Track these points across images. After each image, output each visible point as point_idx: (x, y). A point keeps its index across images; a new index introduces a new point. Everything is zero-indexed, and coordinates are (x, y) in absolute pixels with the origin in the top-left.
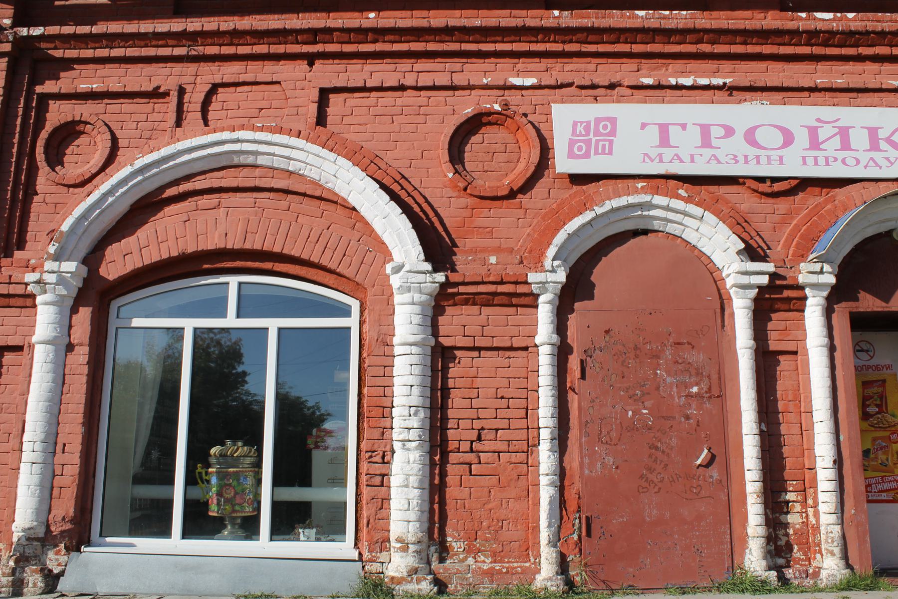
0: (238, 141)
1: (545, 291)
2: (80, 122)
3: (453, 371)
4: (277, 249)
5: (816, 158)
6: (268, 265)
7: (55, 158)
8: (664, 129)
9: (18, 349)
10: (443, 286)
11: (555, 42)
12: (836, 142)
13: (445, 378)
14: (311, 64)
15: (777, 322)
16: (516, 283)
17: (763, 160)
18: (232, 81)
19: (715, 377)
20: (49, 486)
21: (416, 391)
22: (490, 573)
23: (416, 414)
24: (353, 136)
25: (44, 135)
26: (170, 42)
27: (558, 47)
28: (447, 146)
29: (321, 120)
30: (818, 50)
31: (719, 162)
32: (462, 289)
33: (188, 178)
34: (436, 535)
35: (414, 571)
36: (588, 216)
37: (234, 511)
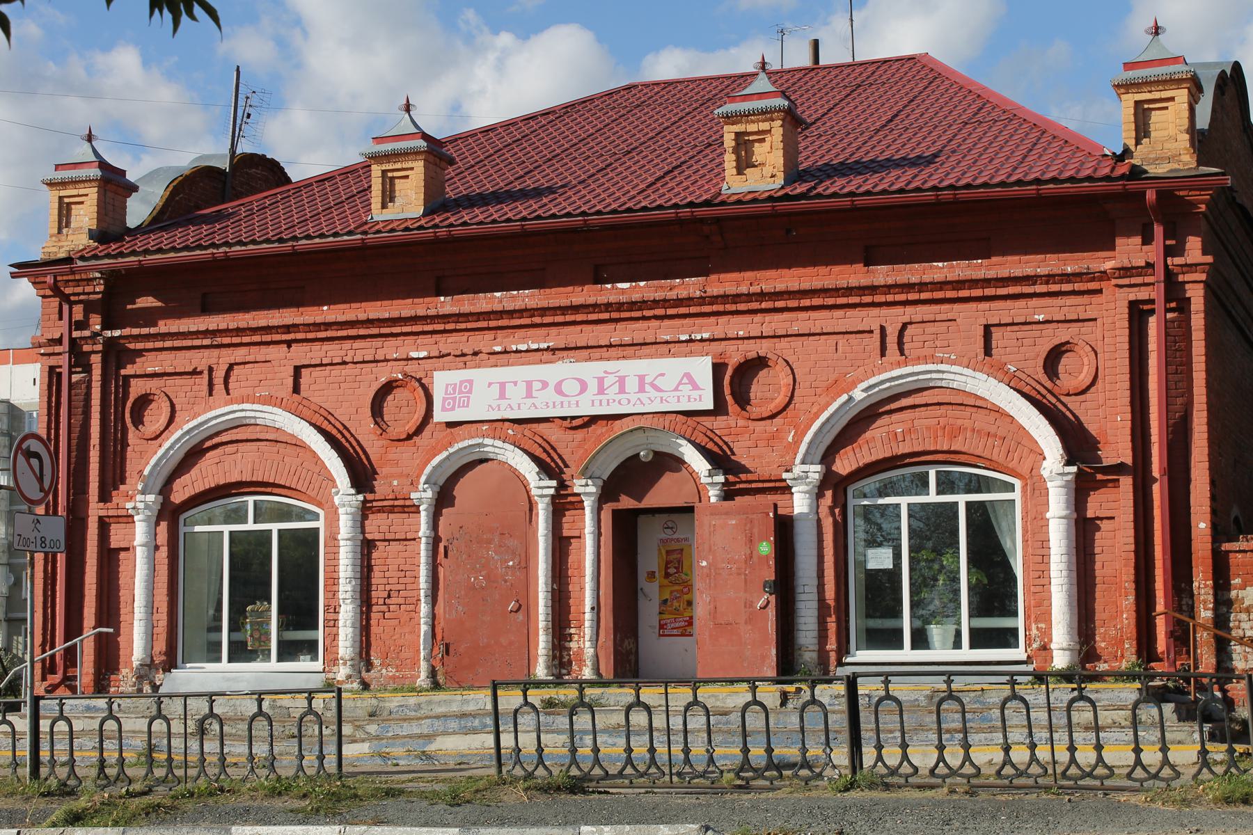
0: (242, 410)
1: (423, 504)
2: (150, 394)
3: (375, 555)
4: (271, 481)
5: (601, 401)
6: (269, 490)
7: (138, 421)
8: (503, 386)
9: (127, 549)
10: (365, 502)
11: (438, 323)
12: (616, 388)
13: (369, 559)
14: (289, 347)
15: (568, 517)
16: (405, 499)
17: (566, 404)
18: (241, 361)
19: (523, 555)
20: (150, 633)
21: (349, 568)
22: (394, 678)
23: (350, 582)
24: (317, 399)
25: (129, 404)
26: (200, 336)
27: (440, 327)
28: (370, 406)
29: (296, 389)
30: (615, 315)
31: (536, 408)
32: (375, 504)
33: (218, 434)
34: (364, 656)
35: (349, 677)
36: (444, 454)
37: (260, 646)
